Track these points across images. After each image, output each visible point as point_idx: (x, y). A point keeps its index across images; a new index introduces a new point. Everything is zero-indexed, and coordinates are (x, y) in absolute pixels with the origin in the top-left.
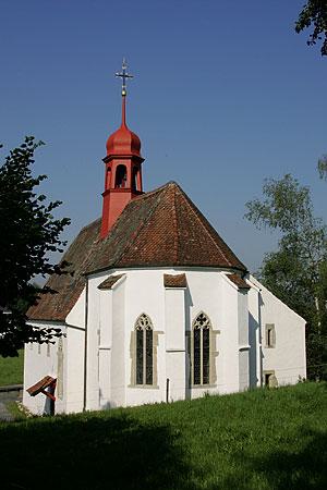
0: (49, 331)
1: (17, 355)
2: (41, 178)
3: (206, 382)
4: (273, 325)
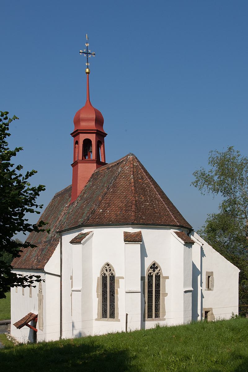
0: (31, 277)
1: (5, 297)
2: (18, 150)
3: (157, 316)
4: (212, 273)
